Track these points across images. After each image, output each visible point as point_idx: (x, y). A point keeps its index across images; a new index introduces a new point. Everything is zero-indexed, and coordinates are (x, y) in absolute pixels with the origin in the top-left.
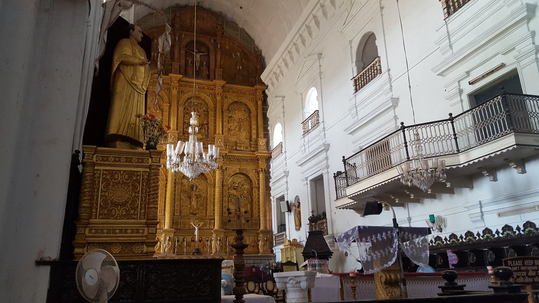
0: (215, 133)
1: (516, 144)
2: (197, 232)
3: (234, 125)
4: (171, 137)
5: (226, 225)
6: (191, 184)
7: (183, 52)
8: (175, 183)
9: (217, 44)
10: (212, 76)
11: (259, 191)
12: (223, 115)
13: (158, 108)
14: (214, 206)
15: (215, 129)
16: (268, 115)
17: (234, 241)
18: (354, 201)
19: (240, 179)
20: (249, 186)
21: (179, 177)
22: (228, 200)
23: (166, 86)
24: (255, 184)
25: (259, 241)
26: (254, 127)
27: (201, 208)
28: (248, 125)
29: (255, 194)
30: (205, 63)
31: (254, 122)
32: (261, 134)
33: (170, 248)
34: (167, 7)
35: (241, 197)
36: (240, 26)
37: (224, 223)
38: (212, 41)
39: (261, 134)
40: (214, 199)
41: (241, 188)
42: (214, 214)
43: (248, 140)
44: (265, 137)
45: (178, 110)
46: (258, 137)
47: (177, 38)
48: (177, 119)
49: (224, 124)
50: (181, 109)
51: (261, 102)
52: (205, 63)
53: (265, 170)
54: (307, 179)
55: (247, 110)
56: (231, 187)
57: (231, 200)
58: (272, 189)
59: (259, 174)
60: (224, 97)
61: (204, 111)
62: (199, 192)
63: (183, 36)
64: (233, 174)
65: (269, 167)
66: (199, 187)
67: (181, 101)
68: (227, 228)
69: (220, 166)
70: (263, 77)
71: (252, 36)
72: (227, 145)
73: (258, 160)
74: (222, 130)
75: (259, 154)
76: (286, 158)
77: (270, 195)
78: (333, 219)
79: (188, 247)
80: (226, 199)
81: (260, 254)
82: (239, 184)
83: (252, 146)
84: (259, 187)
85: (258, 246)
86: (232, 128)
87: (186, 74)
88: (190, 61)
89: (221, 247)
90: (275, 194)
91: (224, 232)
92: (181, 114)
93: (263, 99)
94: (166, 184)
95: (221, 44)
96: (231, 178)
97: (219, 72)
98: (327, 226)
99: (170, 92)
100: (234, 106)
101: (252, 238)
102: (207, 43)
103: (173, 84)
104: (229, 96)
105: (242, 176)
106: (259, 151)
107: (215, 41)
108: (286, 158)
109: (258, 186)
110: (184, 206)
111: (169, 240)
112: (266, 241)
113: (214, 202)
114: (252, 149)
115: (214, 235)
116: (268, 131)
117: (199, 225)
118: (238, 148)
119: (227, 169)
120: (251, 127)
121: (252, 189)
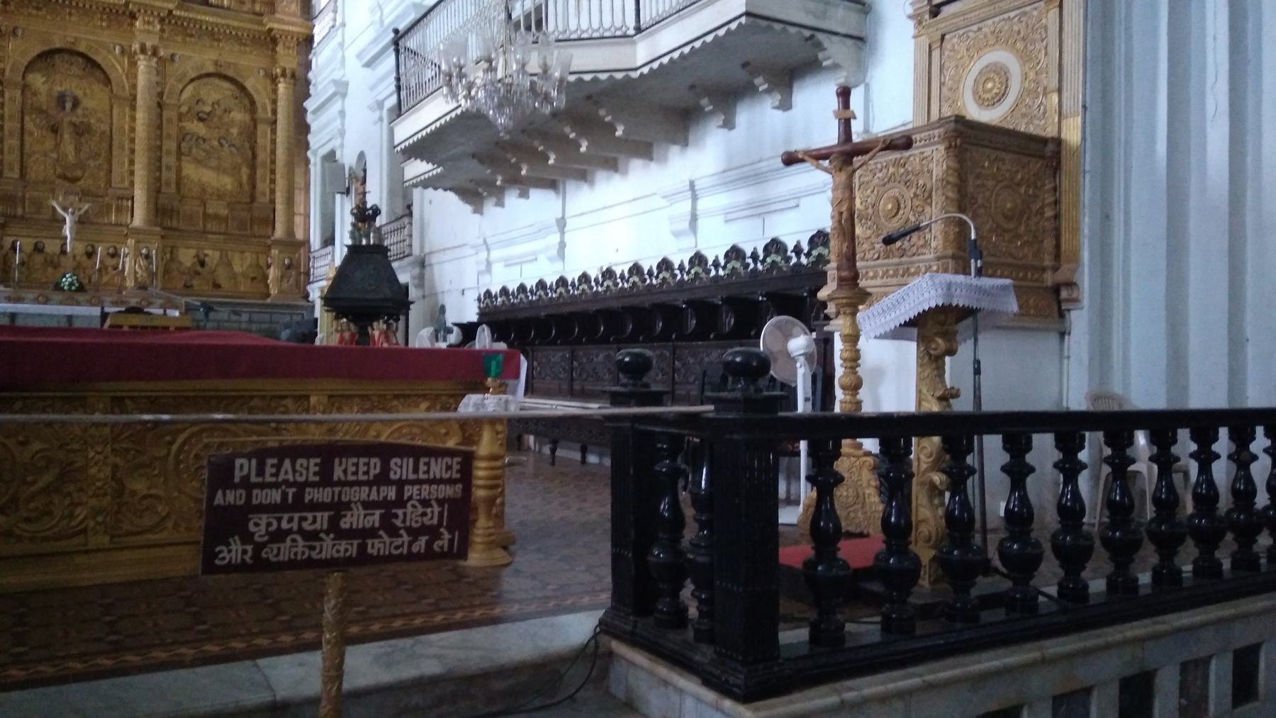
1: (747, 14)
2: (71, 229)
5: (171, 219)
6: (59, 92)
11: (274, 132)
14: (132, 162)
17: (193, 265)
18: (430, 166)
19: (217, 93)
20: (247, 118)
21: (13, 65)
22: (179, 147)
24: (264, 112)
25: (269, 266)
27: (92, 163)
29: (263, 140)
35: (221, 145)
37: (161, 211)
40: (133, 140)
41: (220, 118)
42: (132, 183)
53: (293, 76)
54: (380, 105)
56: (187, 112)
57: (190, 149)
58: (313, 128)
59: (276, 85)
62: (84, 116)
64: (193, 75)
65: (308, 66)
66: (88, 103)
68: (175, 223)
73: (274, 41)
75: (276, 26)
76: (341, 45)
77: (307, 146)
78: (426, 221)
80: (170, 145)
81: (269, 301)
82: (216, 107)
84: (275, 122)
85: (267, 279)
90: (318, 142)
91: (163, 237)
96: (190, 88)
98: (411, 236)
101: (249, 258)
105: (226, 85)
106: (278, 16)
108: (341, 45)
109: (274, 118)
110: (34, 153)
113: (133, 151)
114: (258, 8)
117: (80, 209)
119: (177, 58)
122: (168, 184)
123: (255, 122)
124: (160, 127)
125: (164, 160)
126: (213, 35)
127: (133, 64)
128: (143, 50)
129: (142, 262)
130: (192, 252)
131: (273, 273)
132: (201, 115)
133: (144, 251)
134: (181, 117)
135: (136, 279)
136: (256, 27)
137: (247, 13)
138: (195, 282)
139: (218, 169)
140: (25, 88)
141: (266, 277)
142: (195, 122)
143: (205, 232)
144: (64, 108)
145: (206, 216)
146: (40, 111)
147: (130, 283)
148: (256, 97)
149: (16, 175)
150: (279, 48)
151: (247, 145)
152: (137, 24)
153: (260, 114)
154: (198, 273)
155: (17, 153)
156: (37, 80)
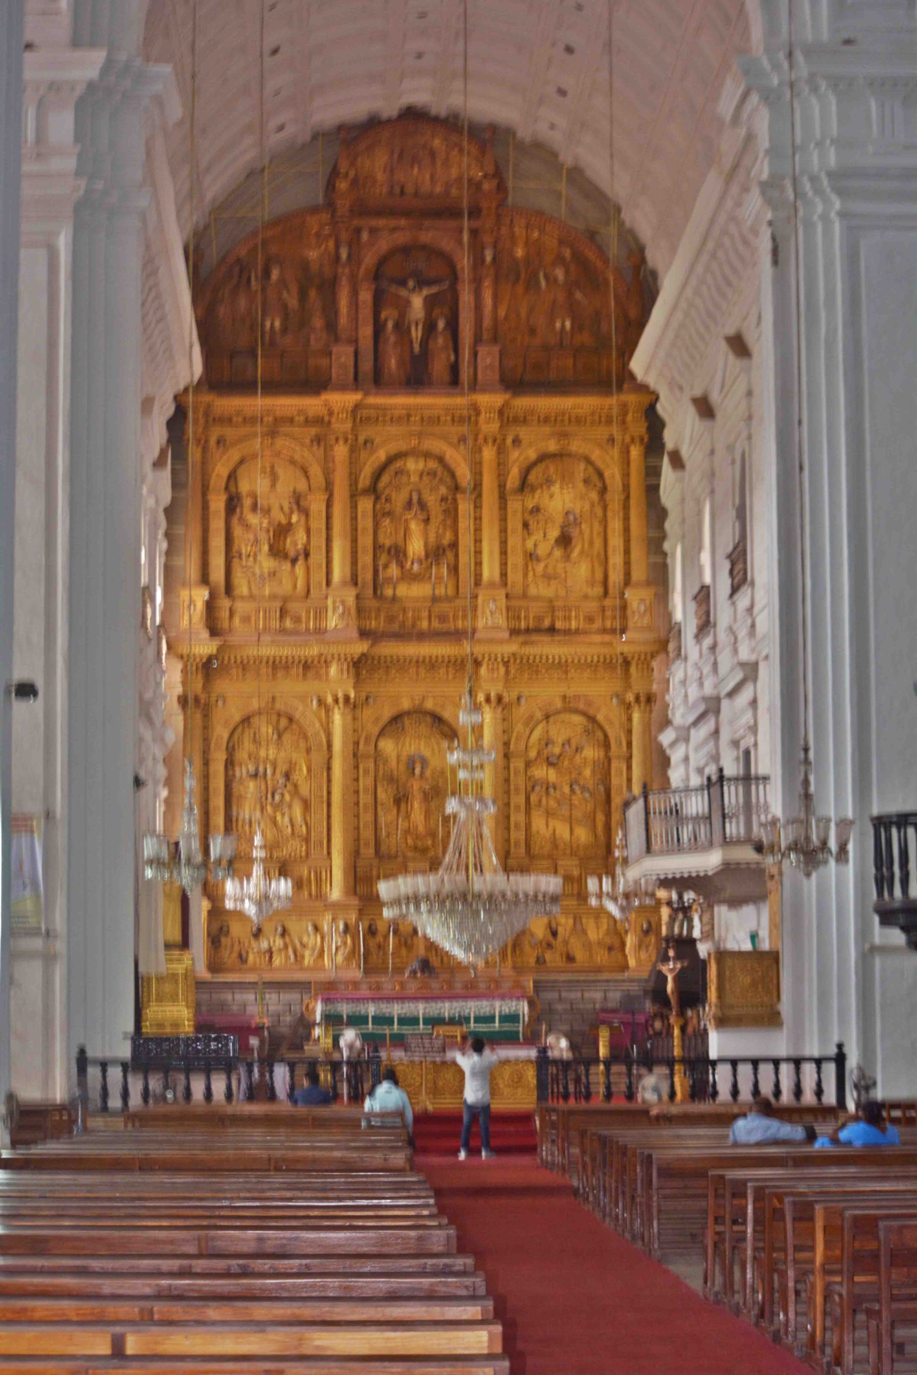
4: (335, 609)
7: (366, 296)
8: (355, 755)
11: (629, 768)
13: (295, 507)
15: (479, 564)
20: (602, 754)
22: (528, 799)
23: (313, 431)
25: (626, 932)
26: (616, 541)
28: (599, 534)
30: (441, 324)
31: (616, 525)
33: (348, 954)
34: (308, 137)
35: (572, 790)
39: (639, 573)
41: (571, 760)
43: (599, 590)
44: (648, 583)
45: (354, 507)
47: (344, 254)
48: (354, 541)
49: (510, 543)
50: (365, 505)
51: (642, 448)
52: (441, 324)
55: (595, 478)
60: (509, 441)
61: (444, 499)
63: (365, 236)
67: (364, 480)
69: (493, 695)
70: (637, 364)
72: (519, 618)
73: (627, 663)
74: (504, 564)
79: (404, 952)
80: (518, 800)
83: (609, 613)
86: (542, 551)
88: (390, 325)
92: (366, 523)
93: (646, 440)
94: (330, 758)
95: (495, 245)
97: (488, 356)
99: (328, 450)
100: (547, 467)
102: (446, 244)
105: (577, 719)
112: (647, 932)
114: (608, 624)
118: (559, 625)
119: (523, 701)
122: (517, 844)
123: (609, 760)
124: (507, 781)
125: (512, 819)
128: (488, 700)
130: (545, 920)
134: (528, 764)
138: (548, 956)
139: (571, 821)
140: (378, 756)
141: (623, 944)
142: (545, 768)
144: (414, 774)
146: (391, 779)
149: (371, 851)
150: (633, 669)
152: (483, 671)
155: (371, 827)
156: (388, 746)
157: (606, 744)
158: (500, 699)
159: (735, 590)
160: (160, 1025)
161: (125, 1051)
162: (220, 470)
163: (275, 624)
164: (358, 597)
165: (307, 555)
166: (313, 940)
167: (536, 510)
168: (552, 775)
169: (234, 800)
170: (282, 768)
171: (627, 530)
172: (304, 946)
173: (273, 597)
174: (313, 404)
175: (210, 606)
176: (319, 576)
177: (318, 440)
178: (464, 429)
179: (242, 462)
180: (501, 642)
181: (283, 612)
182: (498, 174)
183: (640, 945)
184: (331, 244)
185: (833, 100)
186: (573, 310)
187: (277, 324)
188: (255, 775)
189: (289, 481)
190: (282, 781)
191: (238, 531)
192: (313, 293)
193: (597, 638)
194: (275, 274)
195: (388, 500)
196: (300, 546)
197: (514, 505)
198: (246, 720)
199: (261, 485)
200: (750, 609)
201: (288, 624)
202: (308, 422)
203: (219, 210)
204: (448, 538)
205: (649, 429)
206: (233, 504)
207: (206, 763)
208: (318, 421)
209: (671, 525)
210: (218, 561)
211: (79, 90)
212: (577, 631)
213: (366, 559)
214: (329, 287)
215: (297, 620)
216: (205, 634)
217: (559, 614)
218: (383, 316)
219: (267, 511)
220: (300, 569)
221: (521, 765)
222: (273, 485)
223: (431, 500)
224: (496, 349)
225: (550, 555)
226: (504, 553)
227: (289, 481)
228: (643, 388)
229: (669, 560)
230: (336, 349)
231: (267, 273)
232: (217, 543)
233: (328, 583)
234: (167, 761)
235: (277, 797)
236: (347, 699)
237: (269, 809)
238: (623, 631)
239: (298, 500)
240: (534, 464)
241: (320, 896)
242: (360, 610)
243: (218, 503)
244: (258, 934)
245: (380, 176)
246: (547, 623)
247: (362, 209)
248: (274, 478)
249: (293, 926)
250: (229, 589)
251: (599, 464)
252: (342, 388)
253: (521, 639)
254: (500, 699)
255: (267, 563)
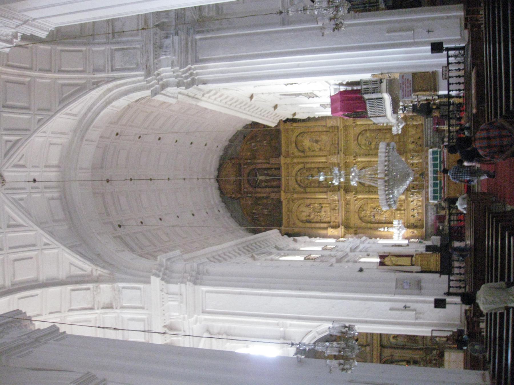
0: (325, 162)
3: (316, 147)
4: (333, 197)
7: (259, 190)
8: (369, 192)
9: (247, 162)
10: (276, 166)
12: (308, 156)
15: (322, 162)
16: (305, 117)
23: (291, 202)
30: (266, 172)
32: (323, 123)
36: (227, 143)
38: (245, 166)
43: (328, 133)
45: (309, 192)
46: (325, 126)
48: (317, 192)
50: (308, 190)
52: (266, 172)
61: (307, 171)
63: (245, 190)
68: (402, 150)
70: (273, 125)
71: (235, 133)
74: (322, 156)
86: (319, 147)
87: (279, 186)
88: (266, 184)
89: (418, 155)
92: (313, 190)
93: (291, 122)
94: (370, 198)
97: (272, 161)
101: (410, 129)
103: (289, 197)
104: (291, 152)
105: (360, 138)
106: (338, 125)
107: (244, 165)
111: (412, 194)
112: (413, 119)
114: (336, 130)
115: (409, 161)
116: (319, 117)
118: (337, 142)
120: (316, 132)
121: (369, 130)
126: (347, 141)
127: (359, 162)
128: (355, 160)
129: (414, 158)
130: (410, 144)
131: (415, 123)
132: (370, 143)
133: (411, 157)
134: (371, 149)
135: (419, 159)
136: (342, 131)
137: (338, 133)
141: (416, 125)
143: (404, 142)
145: (399, 142)
147: (421, 161)
148: (363, 129)
151: (377, 131)
152: (348, 161)
153: (367, 128)
154: (416, 143)
157: (366, 130)
158: (354, 157)
159: (317, 97)
160: (437, 265)
161: (445, 277)
162: (300, 224)
163: (337, 211)
164: (330, 192)
165: (320, 204)
166: (415, 202)
167: (309, 148)
168: (374, 144)
169: (380, 221)
170: (372, 210)
171: (314, 126)
172: (417, 205)
173: (330, 212)
174: (284, 203)
175: (333, 227)
176: (325, 201)
177: (293, 201)
178: (290, 166)
179: (298, 219)
180: (341, 157)
181: (334, 209)
182: (231, 159)
183: (416, 121)
184: (247, 198)
185: (161, 69)
186: (261, 141)
187: (266, 211)
188: (374, 216)
189: (303, 208)
190: (375, 210)
191: (315, 220)
192: (259, 202)
193: (339, 133)
194: (254, 211)
195: (307, 184)
196: (318, 205)
197: (308, 154)
198: (361, 219)
199: (304, 214)
200: (320, 91)
201: (337, 208)
202: (289, 203)
203: (241, 224)
204: (316, 170)
205: (289, 122)
206: (309, 222)
207: (371, 228)
208: (288, 201)
209: (312, 116)
210: (322, 225)
211: (163, 282)
212: (338, 138)
213: (321, 190)
214: (257, 199)
215: (336, 206)
216: (339, 229)
217: (334, 142)
218: (263, 185)
219: (310, 213)
220: (324, 205)
221: (371, 151)
222: (304, 212)
223: (307, 174)
224: (271, 159)
225: (320, 145)
226: (320, 156)
227: (303, 208)
228: (279, 123)
229: (320, 116)
230: (271, 197)
231: (254, 213)
232: (317, 225)
233: (327, 199)
234: (371, 238)
235: (380, 211)
236: (354, 194)
237: (383, 213)
238: (338, 127)
239: (308, 206)
240: (298, 148)
241: (404, 200)
242: (333, 191)
243: (308, 225)
244: (414, 217)
245: (232, 187)
246: (336, 145)
247: (239, 191)
248: (302, 211)
249: (411, 207)
250: (329, 222)
251: (298, 133)
252: (280, 196)
253: (340, 152)
254: (354, 157)
255: (323, 213)
